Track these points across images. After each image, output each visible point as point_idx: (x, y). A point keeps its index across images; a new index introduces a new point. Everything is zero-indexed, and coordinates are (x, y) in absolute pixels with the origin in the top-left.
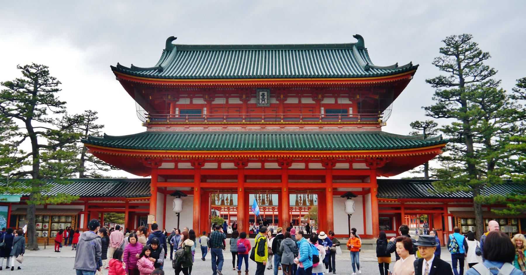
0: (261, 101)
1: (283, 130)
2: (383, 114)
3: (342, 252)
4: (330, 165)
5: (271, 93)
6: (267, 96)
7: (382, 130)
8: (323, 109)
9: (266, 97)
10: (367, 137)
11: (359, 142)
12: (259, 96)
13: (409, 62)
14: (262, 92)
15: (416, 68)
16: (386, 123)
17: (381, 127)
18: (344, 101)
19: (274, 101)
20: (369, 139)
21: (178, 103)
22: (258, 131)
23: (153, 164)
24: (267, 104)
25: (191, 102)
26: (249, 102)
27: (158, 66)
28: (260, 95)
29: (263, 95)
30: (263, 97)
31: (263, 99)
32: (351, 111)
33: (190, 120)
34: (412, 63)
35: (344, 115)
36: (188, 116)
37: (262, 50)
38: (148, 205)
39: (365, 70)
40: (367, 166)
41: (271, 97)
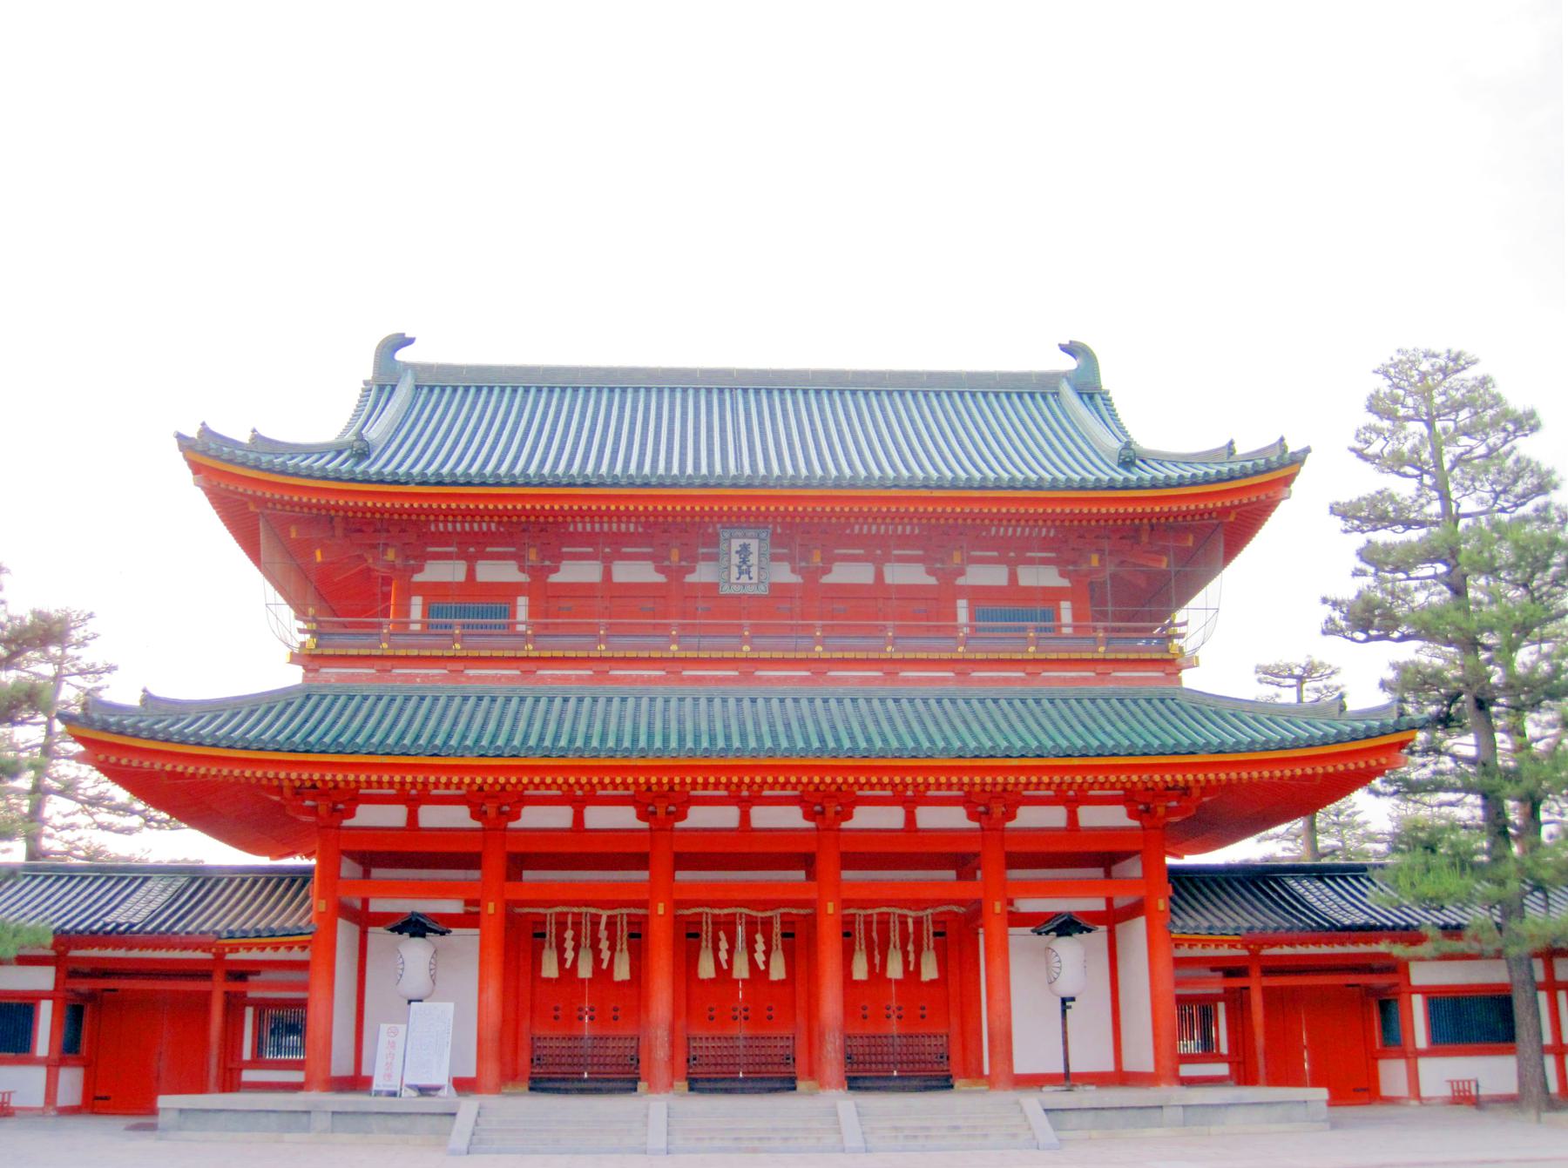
0: (735, 572)
2: (1185, 624)
3: (1060, 1140)
4: (998, 810)
5: (773, 545)
6: (760, 555)
9: (753, 559)
10: (1132, 707)
11: (1109, 728)
12: (729, 553)
14: (742, 541)
15: (1298, 460)
16: (1197, 658)
17: (1180, 670)
18: (1047, 577)
19: (784, 574)
20: (1141, 716)
21: (418, 578)
23: (322, 809)
24: (757, 585)
25: (471, 573)
26: (690, 578)
27: (350, 437)
28: (733, 553)
29: (745, 548)
30: (744, 561)
31: (744, 567)
32: (1066, 610)
33: (468, 640)
35: (1046, 629)
36: (463, 626)
37: (731, 390)
39: (1119, 466)
40: (1131, 815)
41: (775, 558)
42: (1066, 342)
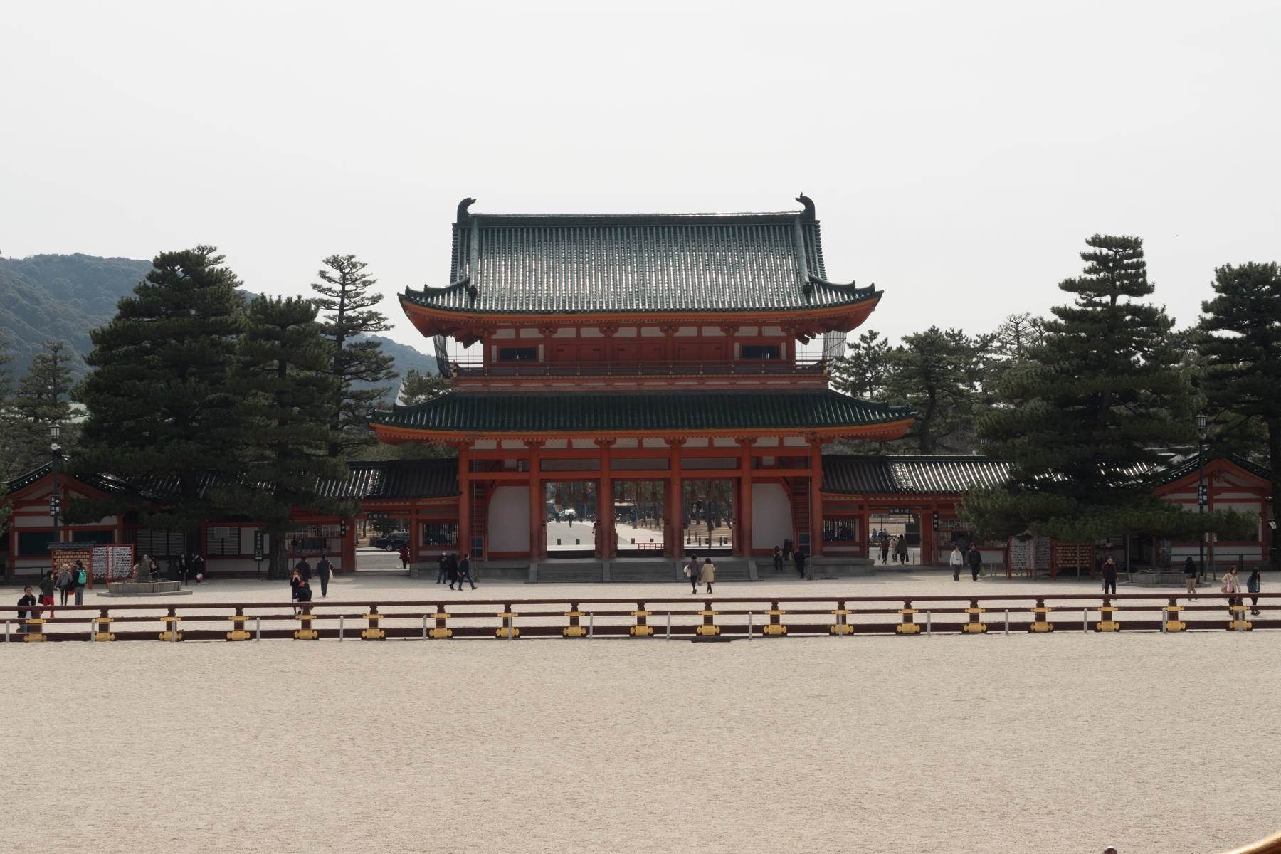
1: (673, 388)
13: (867, 285)
15: (880, 294)
21: (494, 337)
22: (632, 389)
34: (875, 285)
38: (456, 507)
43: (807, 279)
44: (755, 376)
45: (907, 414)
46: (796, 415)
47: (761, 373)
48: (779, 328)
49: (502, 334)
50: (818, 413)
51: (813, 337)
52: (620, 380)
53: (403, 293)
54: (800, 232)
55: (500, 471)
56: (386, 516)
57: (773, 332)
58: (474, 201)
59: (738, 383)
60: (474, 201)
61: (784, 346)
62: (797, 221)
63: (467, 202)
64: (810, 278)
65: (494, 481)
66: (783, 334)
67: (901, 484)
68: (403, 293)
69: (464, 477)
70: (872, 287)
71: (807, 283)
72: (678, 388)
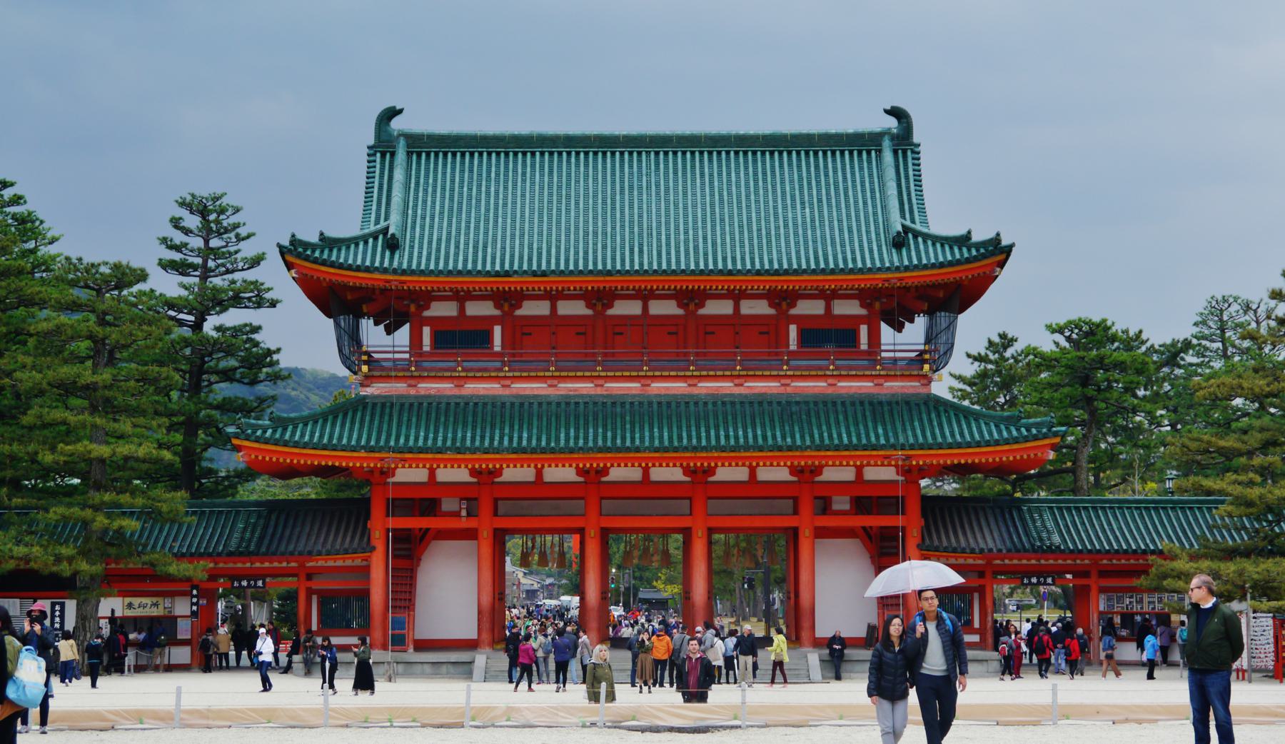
1: (695, 391)
7: (933, 392)
8: (793, 330)
21: (426, 313)
22: (634, 392)
38: (366, 570)
42: (889, 108)
43: (900, 228)
44: (820, 373)
45: (1049, 430)
46: (880, 431)
47: (828, 369)
48: (857, 302)
49: (443, 309)
50: (913, 430)
51: (912, 321)
52: (615, 378)
53: (286, 243)
54: (888, 156)
55: (435, 516)
56: (260, 583)
57: (848, 308)
58: (400, 111)
59: (793, 384)
60: (400, 111)
61: (864, 330)
62: (887, 144)
63: (392, 113)
64: (903, 226)
65: (428, 530)
66: (863, 312)
67: (1041, 539)
68: (286, 243)
69: (381, 525)
70: (997, 240)
71: (899, 233)
72: (704, 391)
